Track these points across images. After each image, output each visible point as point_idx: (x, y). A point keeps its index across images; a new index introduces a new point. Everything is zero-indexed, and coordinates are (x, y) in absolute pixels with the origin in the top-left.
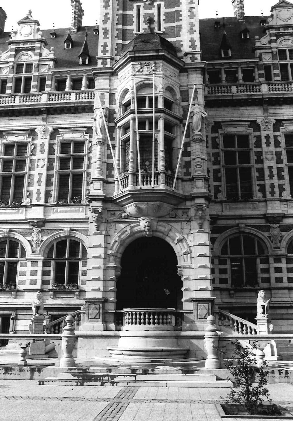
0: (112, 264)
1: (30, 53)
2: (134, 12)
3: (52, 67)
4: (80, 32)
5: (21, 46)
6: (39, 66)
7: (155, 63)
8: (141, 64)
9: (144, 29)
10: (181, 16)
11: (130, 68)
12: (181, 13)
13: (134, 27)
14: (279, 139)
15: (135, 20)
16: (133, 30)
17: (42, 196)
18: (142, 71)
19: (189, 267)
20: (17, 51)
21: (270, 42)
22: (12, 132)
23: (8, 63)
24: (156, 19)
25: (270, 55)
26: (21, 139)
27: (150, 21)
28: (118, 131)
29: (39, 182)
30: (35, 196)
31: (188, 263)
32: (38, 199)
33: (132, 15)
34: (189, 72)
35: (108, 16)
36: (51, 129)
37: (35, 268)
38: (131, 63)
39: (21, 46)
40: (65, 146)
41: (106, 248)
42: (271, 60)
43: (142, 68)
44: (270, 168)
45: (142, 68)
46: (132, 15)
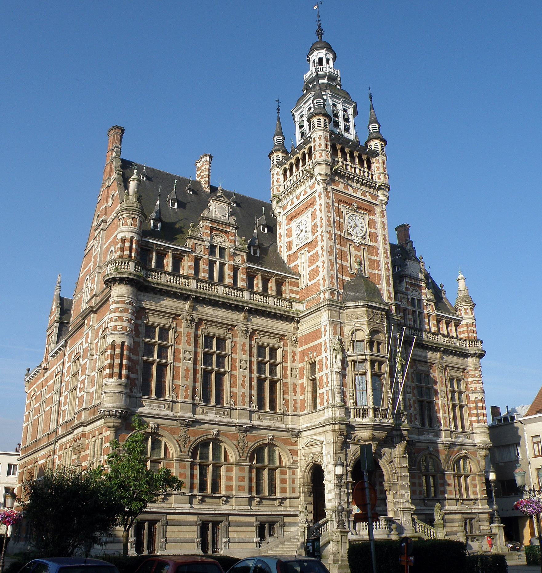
0: (350, 480)
1: (223, 235)
3: (246, 261)
5: (216, 226)
6: (234, 253)
7: (382, 314)
8: (373, 312)
9: (356, 269)
14: (413, 375)
15: (348, 257)
17: (247, 399)
19: (397, 483)
20: (212, 229)
21: (407, 289)
22: (213, 323)
23: (204, 241)
25: (406, 300)
26: (221, 332)
28: (350, 365)
29: (243, 385)
30: (239, 399)
31: (395, 481)
32: (243, 402)
36: (251, 330)
37: (242, 474)
38: (365, 309)
39: (216, 226)
40: (261, 348)
41: (346, 466)
42: (407, 305)
44: (409, 400)
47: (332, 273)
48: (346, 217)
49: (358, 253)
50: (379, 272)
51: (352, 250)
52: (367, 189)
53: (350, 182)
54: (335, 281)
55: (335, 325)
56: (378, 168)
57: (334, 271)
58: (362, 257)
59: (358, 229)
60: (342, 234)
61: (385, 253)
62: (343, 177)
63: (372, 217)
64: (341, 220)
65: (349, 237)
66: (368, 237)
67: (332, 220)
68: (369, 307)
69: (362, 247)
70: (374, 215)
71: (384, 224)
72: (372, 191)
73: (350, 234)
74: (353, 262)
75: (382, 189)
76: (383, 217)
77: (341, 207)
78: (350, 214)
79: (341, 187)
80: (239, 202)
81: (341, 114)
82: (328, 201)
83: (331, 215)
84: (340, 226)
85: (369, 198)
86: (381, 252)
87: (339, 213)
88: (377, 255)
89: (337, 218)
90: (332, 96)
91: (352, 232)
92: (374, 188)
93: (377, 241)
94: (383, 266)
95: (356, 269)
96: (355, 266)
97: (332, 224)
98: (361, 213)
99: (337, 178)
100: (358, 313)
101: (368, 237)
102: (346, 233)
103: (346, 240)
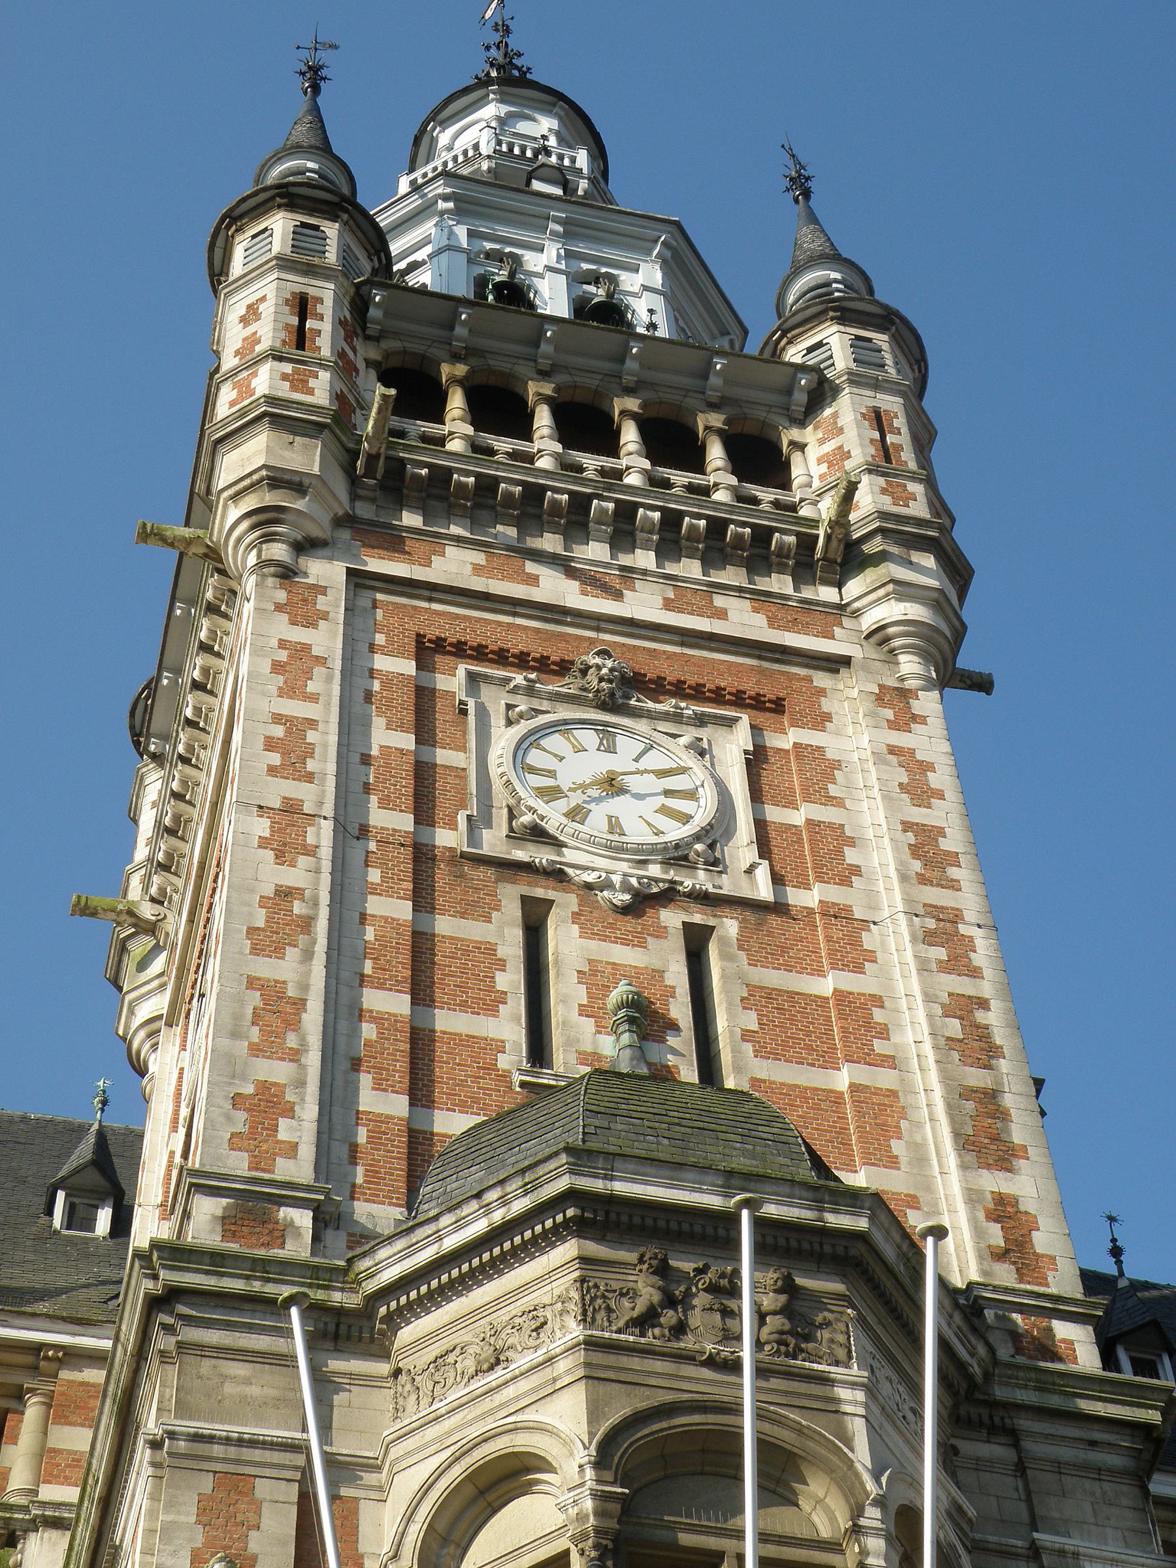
8: (663, 1270)
10: (884, 1033)
11: (565, 1283)
12: (878, 1015)
13: (508, 1028)
18: (680, 1329)
24: (680, 1010)
27: (644, 1019)
34: (1028, 1445)
35: (298, 908)
38: (567, 1250)
43: (670, 1301)
45: (670, 1301)
47: (278, 1071)
50: (884, 1078)
51: (565, 942)
52: (732, 576)
53: (550, 542)
54: (300, 1129)
55: (235, 1486)
57: (295, 1056)
60: (446, 838)
65: (520, 855)
66: (742, 848)
67: (326, 739)
68: (598, 1218)
69: (672, 918)
70: (821, 721)
71: (919, 768)
72: (780, 583)
73: (537, 834)
75: (881, 557)
79: (455, 565)
82: (299, 635)
85: (743, 620)
86: (895, 943)
92: (805, 563)
93: (847, 875)
96: (586, 1039)
98: (676, 717)
99: (411, 519)
100: (503, 1316)
101: (742, 848)
103: (490, 872)
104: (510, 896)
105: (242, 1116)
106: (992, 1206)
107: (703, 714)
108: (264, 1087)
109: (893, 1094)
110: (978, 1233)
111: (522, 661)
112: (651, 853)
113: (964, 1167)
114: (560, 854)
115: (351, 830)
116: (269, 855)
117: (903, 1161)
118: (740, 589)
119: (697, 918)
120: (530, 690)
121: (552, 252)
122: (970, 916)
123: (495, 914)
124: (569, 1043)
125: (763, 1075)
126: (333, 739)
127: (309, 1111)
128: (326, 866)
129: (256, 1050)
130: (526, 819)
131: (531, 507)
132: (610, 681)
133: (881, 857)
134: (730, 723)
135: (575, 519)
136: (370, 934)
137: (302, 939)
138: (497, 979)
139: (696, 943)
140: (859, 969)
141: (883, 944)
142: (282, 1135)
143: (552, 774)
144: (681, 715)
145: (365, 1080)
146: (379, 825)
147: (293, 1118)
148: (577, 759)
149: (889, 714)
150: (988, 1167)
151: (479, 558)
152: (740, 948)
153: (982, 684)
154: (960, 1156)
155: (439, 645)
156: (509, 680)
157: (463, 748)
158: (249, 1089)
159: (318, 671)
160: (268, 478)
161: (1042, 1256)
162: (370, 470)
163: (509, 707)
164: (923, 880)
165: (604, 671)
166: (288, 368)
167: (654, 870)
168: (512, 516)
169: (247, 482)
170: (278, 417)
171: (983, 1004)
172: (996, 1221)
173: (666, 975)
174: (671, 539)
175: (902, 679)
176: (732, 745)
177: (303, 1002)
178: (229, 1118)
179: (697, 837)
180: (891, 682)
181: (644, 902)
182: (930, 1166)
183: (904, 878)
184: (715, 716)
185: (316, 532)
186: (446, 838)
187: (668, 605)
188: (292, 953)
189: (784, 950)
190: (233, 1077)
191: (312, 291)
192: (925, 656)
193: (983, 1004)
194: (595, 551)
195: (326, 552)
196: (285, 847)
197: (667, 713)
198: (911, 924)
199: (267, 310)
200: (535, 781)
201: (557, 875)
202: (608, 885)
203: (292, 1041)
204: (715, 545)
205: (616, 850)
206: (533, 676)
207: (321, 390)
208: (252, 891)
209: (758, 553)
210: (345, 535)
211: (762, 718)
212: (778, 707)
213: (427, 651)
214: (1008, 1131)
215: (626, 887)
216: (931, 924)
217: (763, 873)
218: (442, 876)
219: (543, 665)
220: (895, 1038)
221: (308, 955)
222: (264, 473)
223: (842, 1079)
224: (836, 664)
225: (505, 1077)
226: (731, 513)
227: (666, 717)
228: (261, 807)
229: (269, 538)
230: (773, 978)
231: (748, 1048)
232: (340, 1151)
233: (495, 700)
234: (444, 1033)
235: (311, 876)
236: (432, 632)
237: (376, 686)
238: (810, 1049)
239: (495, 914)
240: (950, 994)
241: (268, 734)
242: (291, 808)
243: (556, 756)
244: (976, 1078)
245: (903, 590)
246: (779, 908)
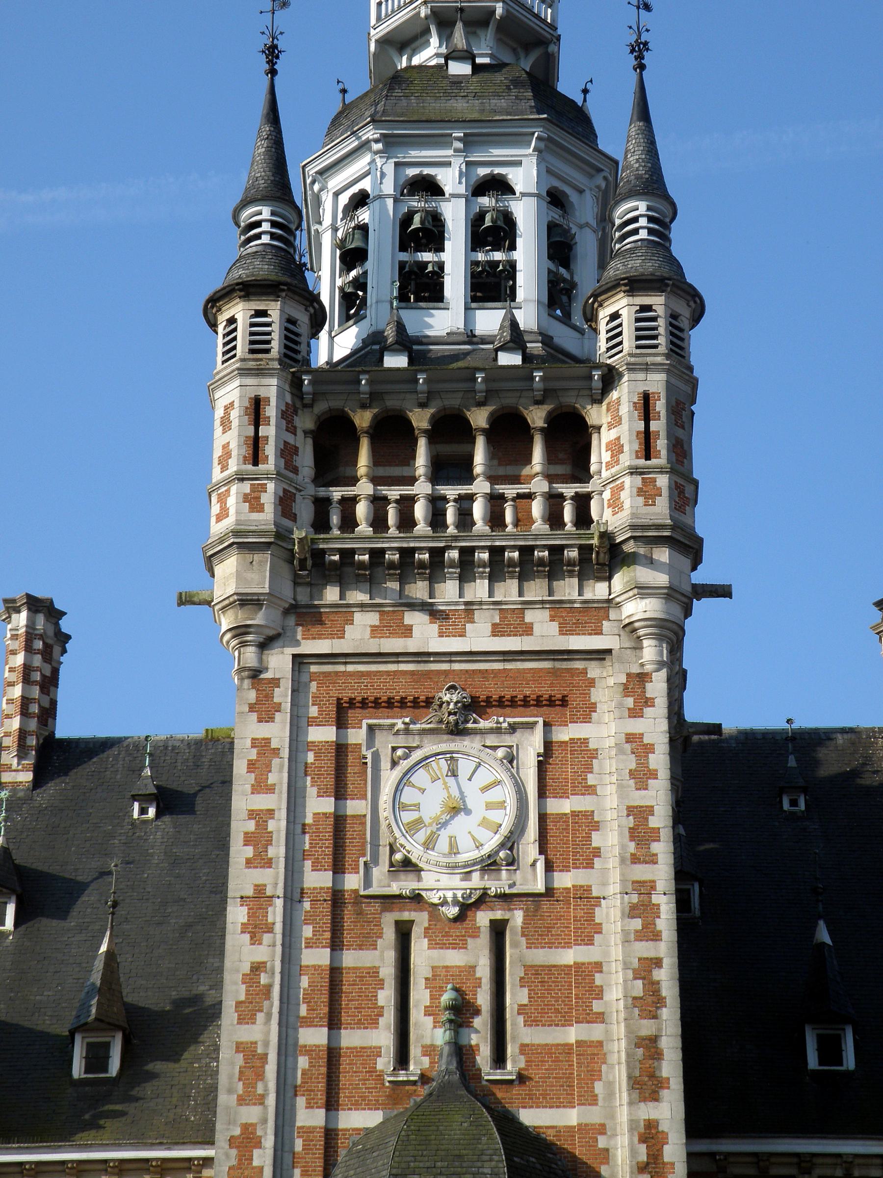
2: (384, 959)
4: (52, 789)
10: (599, 993)
12: (598, 979)
13: (383, 1037)
15: (386, 997)
16: (377, 1052)
24: (483, 999)
27: (461, 1013)
33: (374, 972)
35: (264, 979)
46: (374, 972)
47: (250, 1114)
48: (389, 778)
49: (454, 958)
50: (595, 1032)
52: (536, 590)
53: (419, 590)
56: (616, 448)
57: (261, 1100)
58: (484, 971)
59: (461, 826)
60: (352, 882)
61: (641, 909)
62: (372, 570)
63: (563, 734)
64: (355, 807)
65: (395, 888)
66: (529, 849)
67: (278, 826)
69: (483, 918)
72: (568, 589)
73: (408, 866)
74: (417, 1015)
75: (630, 560)
76: (635, 713)
77: (357, 736)
78: (417, 755)
80: (188, 785)
81: (455, 216)
83: (277, 802)
84: (341, 842)
87: (342, 771)
88: (588, 932)
89: (318, 805)
90: (390, 143)
91: (416, 853)
94: (616, 990)
95: (429, 1050)
96: (429, 1032)
97: (278, 851)
98: (498, 731)
99: (331, 594)
101: (529, 849)
102: (380, 872)
104: (388, 921)
105: (234, 1152)
106: (642, 1131)
107: (515, 723)
108: (246, 1127)
109: (600, 1044)
110: (633, 1152)
111: (403, 703)
112: (474, 865)
113: (631, 1103)
114: (419, 879)
115: (294, 894)
116: (247, 937)
117: (600, 1097)
118: (543, 602)
119: (498, 915)
120: (407, 731)
121: (458, 163)
122: (661, 886)
123: (379, 941)
124: (417, 1041)
125: (527, 1041)
126: (284, 823)
127: (269, 1142)
128: (279, 941)
129: (241, 1101)
130: (398, 857)
131: (406, 565)
132: (455, 714)
133: (611, 839)
134: (531, 726)
135: (435, 568)
136: (305, 982)
137: (266, 1003)
138: (379, 997)
139: (498, 930)
140: (590, 942)
141: (608, 914)
142: (255, 1163)
143: (417, 807)
144: (500, 728)
145: (301, 1101)
146: (312, 886)
147: (261, 1148)
148: (429, 795)
149: (630, 702)
150: (643, 1099)
151: (373, 618)
152: (523, 935)
153: (723, 592)
154: (629, 1095)
155: (351, 702)
156: (393, 725)
157: (364, 797)
158: (237, 1132)
159: (275, 762)
160: (239, 600)
161: (667, 1164)
162: (303, 567)
163: (394, 749)
164: (635, 859)
165: (452, 706)
166: (246, 487)
167: (476, 881)
168: (395, 574)
169: (227, 602)
170: (243, 543)
171: (657, 963)
172: (644, 1142)
173: (478, 969)
174: (498, 568)
175: (642, 665)
176: (531, 746)
177: (266, 1055)
178: (227, 1156)
179: (502, 846)
180: (635, 670)
181: (466, 909)
182: (615, 1099)
183: (623, 861)
184: (522, 723)
185: (271, 633)
186: (352, 882)
187: (497, 631)
188: (260, 1017)
189: (549, 929)
190: (230, 1123)
191: (262, 392)
192: (659, 638)
193: (657, 963)
194: (448, 591)
195: (280, 642)
196: (256, 929)
197: (492, 729)
198: (622, 898)
199: (235, 414)
200: (407, 817)
201: (416, 898)
202: (444, 903)
203: (260, 1090)
204: (527, 566)
205: (452, 868)
206: (407, 720)
207: (267, 517)
208: (238, 971)
209: (555, 566)
210: (291, 620)
211: (553, 713)
212: (564, 702)
213: (342, 715)
214: (660, 1068)
215: (456, 902)
216: (635, 898)
217: (540, 866)
218: (348, 913)
219: (415, 703)
220: (607, 997)
221: (269, 1016)
222: (236, 597)
223: (572, 1034)
224: (601, 655)
225: (380, 1077)
226: (536, 540)
227: (492, 731)
228: (242, 898)
229: (243, 644)
230: (541, 956)
231: (521, 1019)
232: (288, 1158)
233: (385, 743)
234: (347, 1048)
235: (269, 951)
236: (346, 695)
237: (311, 757)
238: (557, 1011)
239: (379, 941)
240: (640, 959)
241: (246, 830)
242: (260, 890)
243: (420, 789)
244: (647, 1028)
245: (643, 590)
246: (550, 892)
